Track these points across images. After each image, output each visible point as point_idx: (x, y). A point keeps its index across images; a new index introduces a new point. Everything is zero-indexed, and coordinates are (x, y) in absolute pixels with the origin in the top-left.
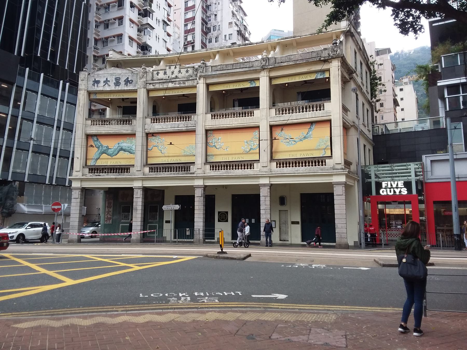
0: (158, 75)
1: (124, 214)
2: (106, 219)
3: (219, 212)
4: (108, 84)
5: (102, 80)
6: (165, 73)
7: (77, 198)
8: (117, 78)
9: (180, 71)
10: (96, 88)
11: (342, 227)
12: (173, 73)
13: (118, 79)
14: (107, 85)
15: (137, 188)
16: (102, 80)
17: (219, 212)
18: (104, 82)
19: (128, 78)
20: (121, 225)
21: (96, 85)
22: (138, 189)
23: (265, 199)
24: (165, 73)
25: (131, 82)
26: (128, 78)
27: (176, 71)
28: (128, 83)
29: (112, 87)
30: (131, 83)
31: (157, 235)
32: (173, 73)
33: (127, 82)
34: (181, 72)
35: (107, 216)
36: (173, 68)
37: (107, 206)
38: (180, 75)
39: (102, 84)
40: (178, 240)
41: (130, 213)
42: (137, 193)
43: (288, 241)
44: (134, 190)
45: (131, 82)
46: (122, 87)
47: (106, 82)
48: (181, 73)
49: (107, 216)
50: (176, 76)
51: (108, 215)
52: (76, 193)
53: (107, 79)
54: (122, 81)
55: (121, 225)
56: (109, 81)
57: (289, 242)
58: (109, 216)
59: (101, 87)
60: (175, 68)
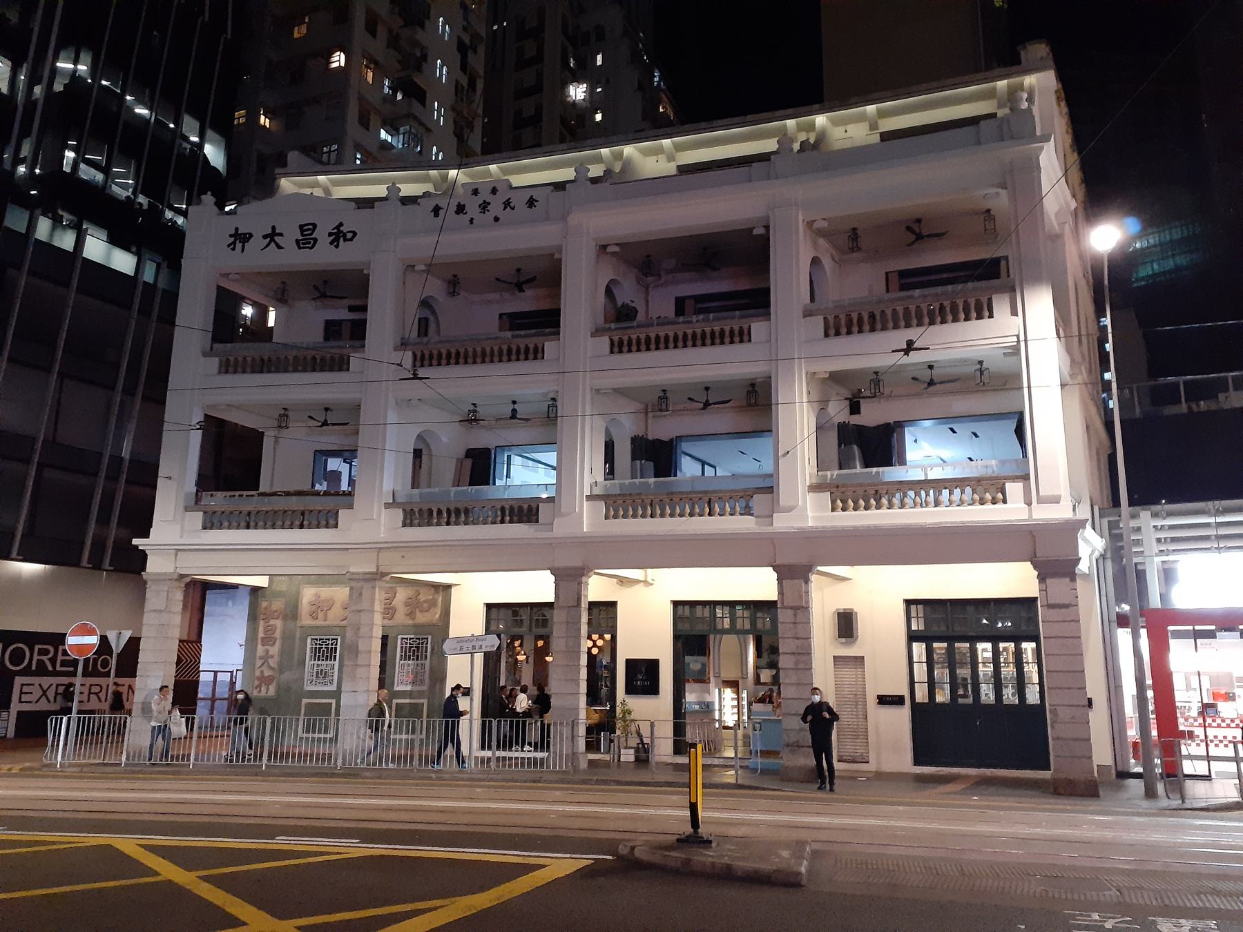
1: (318, 665)
2: (257, 683)
5: (259, 229)
7: (160, 611)
11: (1073, 718)
14: (273, 244)
16: (259, 229)
18: (265, 237)
19: (341, 224)
20: (305, 701)
21: (239, 245)
23: (795, 615)
25: (349, 236)
26: (341, 224)
28: (342, 239)
30: (351, 239)
31: (424, 736)
33: (338, 236)
35: (262, 672)
37: (262, 638)
40: (498, 754)
41: (337, 663)
43: (868, 762)
45: (349, 236)
47: (272, 236)
49: (262, 672)
51: (265, 668)
53: (274, 228)
54: (322, 234)
55: (305, 701)
57: (871, 767)
58: (267, 673)
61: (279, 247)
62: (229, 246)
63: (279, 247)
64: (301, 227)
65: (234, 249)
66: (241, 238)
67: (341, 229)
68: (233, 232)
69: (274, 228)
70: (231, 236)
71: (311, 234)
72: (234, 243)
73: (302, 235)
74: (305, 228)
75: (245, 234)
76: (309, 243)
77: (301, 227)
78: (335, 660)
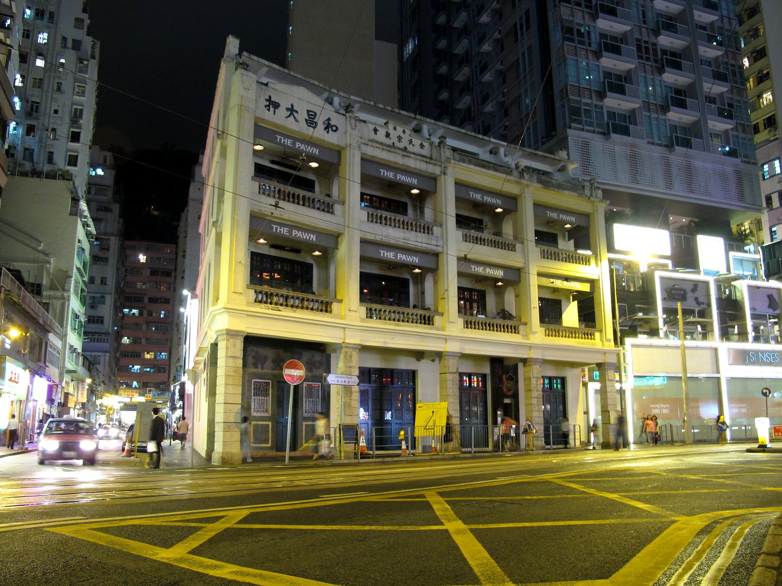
4: (295, 118)
6: (388, 135)
8: (312, 111)
9: (411, 142)
10: (268, 115)
13: (312, 115)
15: (352, 346)
16: (285, 104)
18: (287, 109)
19: (329, 119)
24: (388, 135)
26: (329, 119)
27: (406, 138)
30: (335, 131)
33: (328, 127)
34: (413, 143)
36: (400, 130)
38: (410, 148)
39: (282, 112)
42: (351, 356)
46: (319, 133)
48: (414, 146)
50: (406, 148)
52: (235, 345)
53: (292, 105)
56: (297, 112)
59: (279, 118)
60: (404, 132)
61: (296, 120)
62: (266, 106)
63: (296, 120)
64: (308, 111)
65: (269, 110)
66: (273, 105)
67: (330, 122)
68: (268, 98)
69: (292, 105)
70: (266, 100)
71: (314, 119)
72: (269, 106)
73: (309, 117)
74: (310, 113)
75: (276, 103)
76: (313, 124)
77: (308, 111)
78: (269, 396)
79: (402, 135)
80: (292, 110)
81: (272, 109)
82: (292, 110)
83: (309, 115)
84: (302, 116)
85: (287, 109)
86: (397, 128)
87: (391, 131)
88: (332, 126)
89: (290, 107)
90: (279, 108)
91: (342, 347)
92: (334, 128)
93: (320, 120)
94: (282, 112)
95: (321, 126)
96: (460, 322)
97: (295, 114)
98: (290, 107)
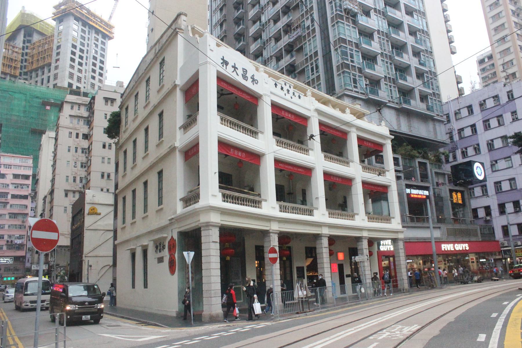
0: (276, 87)
3: (297, 268)
6: (282, 88)
12: (288, 91)
16: (231, 64)
17: (297, 268)
19: (253, 76)
22: (274, 234)
24: (282, 88)
26: (253, 76)
29: (240, 79)
32: (288, 91)
44: (271, 234)
45: (256, 82)
46: (248, 84)
56: (237, 69)
62: (221, 63)
66: (225, 63)
75: (226, 61)
79: (289, 89)
80: (235, 68)
81: (225, 66)
82: (235, 68)
83: (243, 71)
84: (240, 72)
85: (233, 67)
86: (287, 84)
87: (283, 86)
88: (255, 80)
89: (234, 65)
90: (229, 65)
91: (270, 233)
92: (256, 82)
93: (249, 75)
94: (230, 69)
95: (250, 80)
96: (327, 213)
97: (236, 70)
98: (234, 65)
